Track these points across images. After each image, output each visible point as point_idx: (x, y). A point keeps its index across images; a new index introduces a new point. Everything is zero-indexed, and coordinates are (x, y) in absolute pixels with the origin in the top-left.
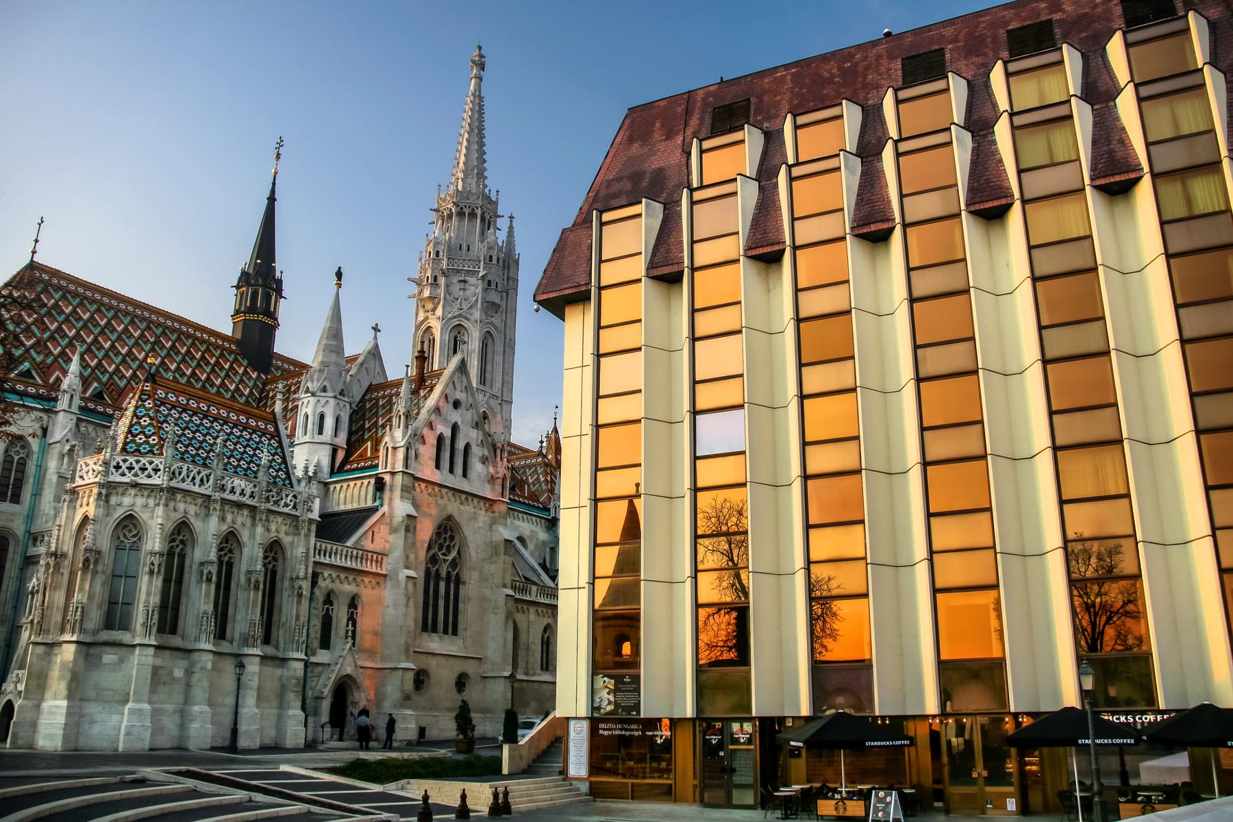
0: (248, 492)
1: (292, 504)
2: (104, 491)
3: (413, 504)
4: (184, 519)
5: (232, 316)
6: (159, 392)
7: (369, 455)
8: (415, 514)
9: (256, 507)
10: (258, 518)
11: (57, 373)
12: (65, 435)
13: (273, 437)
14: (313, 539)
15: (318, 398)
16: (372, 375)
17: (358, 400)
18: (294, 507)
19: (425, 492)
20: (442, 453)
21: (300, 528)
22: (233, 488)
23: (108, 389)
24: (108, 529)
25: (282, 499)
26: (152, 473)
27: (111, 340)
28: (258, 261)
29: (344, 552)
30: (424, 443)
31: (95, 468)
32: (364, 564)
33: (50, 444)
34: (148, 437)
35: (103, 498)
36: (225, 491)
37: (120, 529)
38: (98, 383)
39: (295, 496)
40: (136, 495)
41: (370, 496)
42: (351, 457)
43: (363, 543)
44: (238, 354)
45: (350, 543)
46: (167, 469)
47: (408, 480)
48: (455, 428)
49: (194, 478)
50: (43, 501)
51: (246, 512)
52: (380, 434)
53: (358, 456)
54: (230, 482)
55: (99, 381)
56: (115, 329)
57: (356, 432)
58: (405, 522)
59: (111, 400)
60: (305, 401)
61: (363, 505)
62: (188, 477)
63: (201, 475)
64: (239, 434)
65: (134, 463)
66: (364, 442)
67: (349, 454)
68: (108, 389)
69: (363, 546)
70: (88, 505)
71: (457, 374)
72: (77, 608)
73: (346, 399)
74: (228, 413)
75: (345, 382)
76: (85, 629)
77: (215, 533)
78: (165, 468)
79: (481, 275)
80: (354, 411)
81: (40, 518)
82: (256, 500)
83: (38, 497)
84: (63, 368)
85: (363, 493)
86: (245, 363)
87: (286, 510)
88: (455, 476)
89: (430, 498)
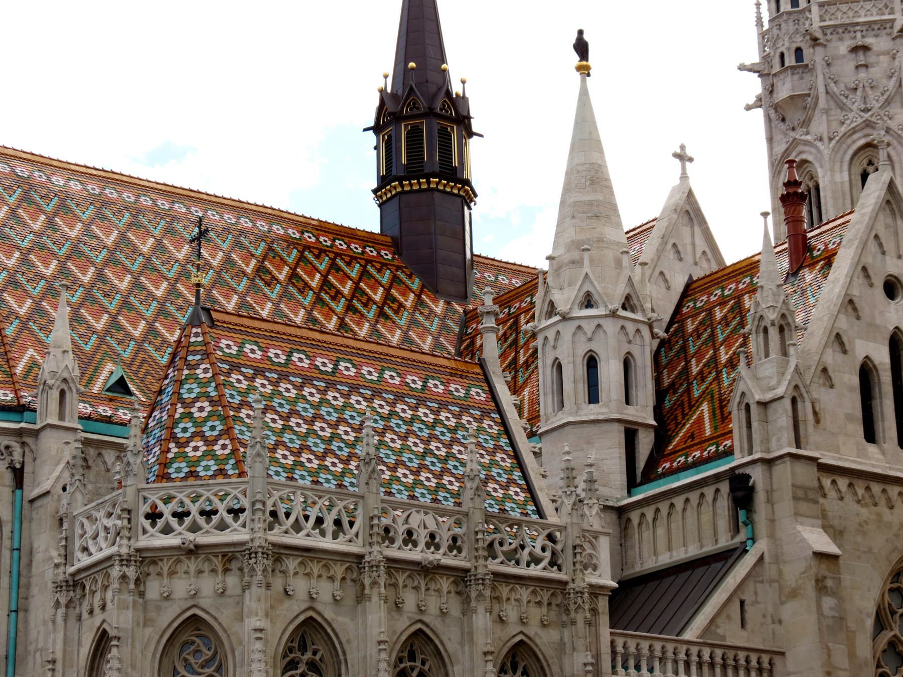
0: (444, 538)
1: (548, 554)
2: (131, 572)
3: (824, 528)
4: (311, 613)
5: (375, 191)
6: (224, 342)
7: (708, 432)
8: (833, 549)
9: (467, 571)
10: (473, 595)
11: (31, 352)
12: (59, 477)
13: (485, 413)
14: (605, 631)
15: (575, 324)
16: (689, 259)
17: (667, 318)
18: (553, 563)
19: (848, 498)
20: (876, 403)
21: (572, 607)
22: (410, 533)
23: (136, 373)
25: (523, 547)
26: (229, 518)
27: (130, 272)
28: (412, 64)
29: (682, 656)
30: (832, 386)
31: (109, 523)
33: (32, 501)
34: (210, 442)
36: (392, 541)
37: (176, 651)
38: (115, 363)
39: (551, 538)
40: (200, 572)
41: (723, 523)
42: (670, 442)
43: (720, 631)
44: (398, 268)
45: (690, 634)
46: (259, 506)
47: (806, 475)
49: (319, 521)
50: (32, 624)
51: (445, 584)
52: (726, 383)
53: (685, 439)
54: (400, 521)
55: (116, 358)
56: (135, 249)
57: (673, 387)
58: (813, 572)
59: (145, 394)
60: (551, 334)
61: (709, 548)
62: (307, 518)
63: (334, 512)
64: (409, 414)
65: (187, 501)
66: (694, 405)
67: (662, 435)
68: (136, 373)
69: (723, 638)
70: (103, 607)
71: (881, 217)
73: (639, 316)
74: (381, 372)
75: (630, 279)
77: (383, 637)
78: (253, 504)
80: (663, 343)
81: (30, 659)
82: (463, 554)
83: (21, 614)
84: (40, 341)
85: (706, 517)
86: (416, 284)
87: (535, 571)
89: (864, 511)
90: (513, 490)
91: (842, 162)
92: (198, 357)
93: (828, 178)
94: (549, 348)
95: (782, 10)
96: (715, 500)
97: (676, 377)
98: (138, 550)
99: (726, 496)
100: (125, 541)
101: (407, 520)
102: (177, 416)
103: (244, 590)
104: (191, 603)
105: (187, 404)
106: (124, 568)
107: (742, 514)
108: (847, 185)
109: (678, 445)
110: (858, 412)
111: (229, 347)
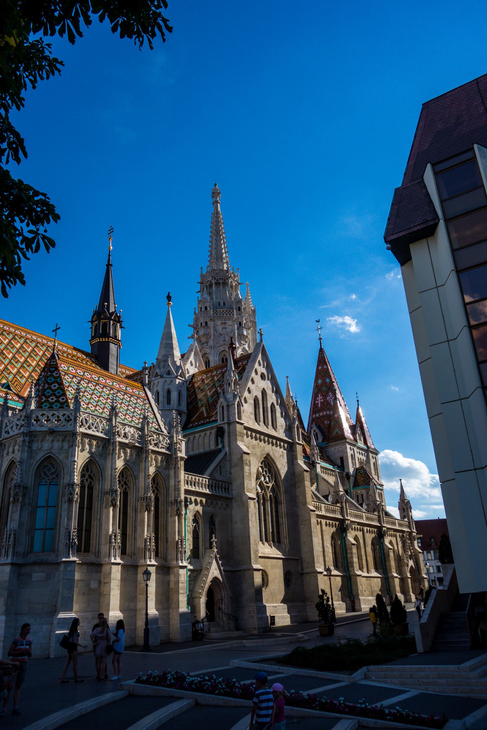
2: (27, 439)
5: (90, 341)
6: (63, 366)
13: (144, 400)
15: (164, 380)
24: (32, 469)
31: (18, 423)
32: (217, 491)
35: (27, 444)
42: (192, 417)
43: (214, 475)
48: (264, 392)
60: (156, 382)
61: (207, 449)
64: (122, 397)
68: (13, 384)
70: (13, 452)
72: (10, 535)
76: (17, 552)
79: (234, 319)
85: (206, 441)
88: (267, 427)
90: (154, 424)
91: (217, 354)
92: (54, 369)
93: (212, 359)
94: (155, 386)
95: (202, 310)
96: (210, 435)
97: (192, 400)
98: (30, 432)
99: (214, 434)
100: (26, 428)
101: (124, 430)
102: (46, 388)
103: (69, 448)
104: (49, 451)
105: (50, 384)
106: (25, 438)
107: (219, 439)
108: (218, 361)
109: (195, 419)
110: (253, 412)
111: (64, 367)
